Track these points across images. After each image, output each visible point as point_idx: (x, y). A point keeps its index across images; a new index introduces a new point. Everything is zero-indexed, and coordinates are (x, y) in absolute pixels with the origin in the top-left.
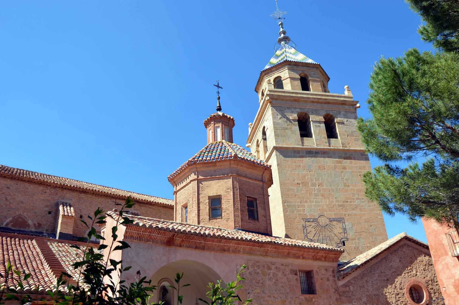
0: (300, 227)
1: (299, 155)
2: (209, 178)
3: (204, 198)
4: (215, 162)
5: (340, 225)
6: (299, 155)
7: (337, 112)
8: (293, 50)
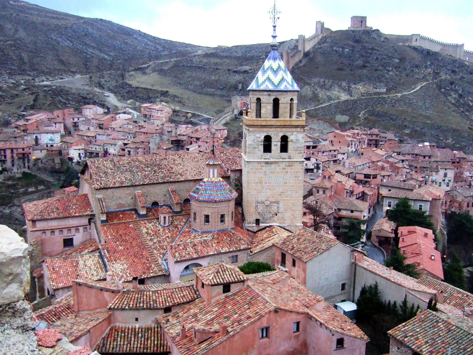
0: (254, 205)
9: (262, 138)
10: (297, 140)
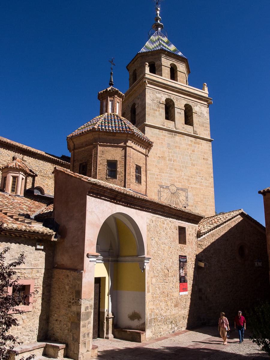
0: (156, 191)
1: (162, 134)
2: (109, 145)
3: (104, 161)
4: (115, 132)
5: (184, 194)
6: (162, 134)
7: (194, 104)
8: (166, 39)
9: (163, 100)
10: (201, 113)
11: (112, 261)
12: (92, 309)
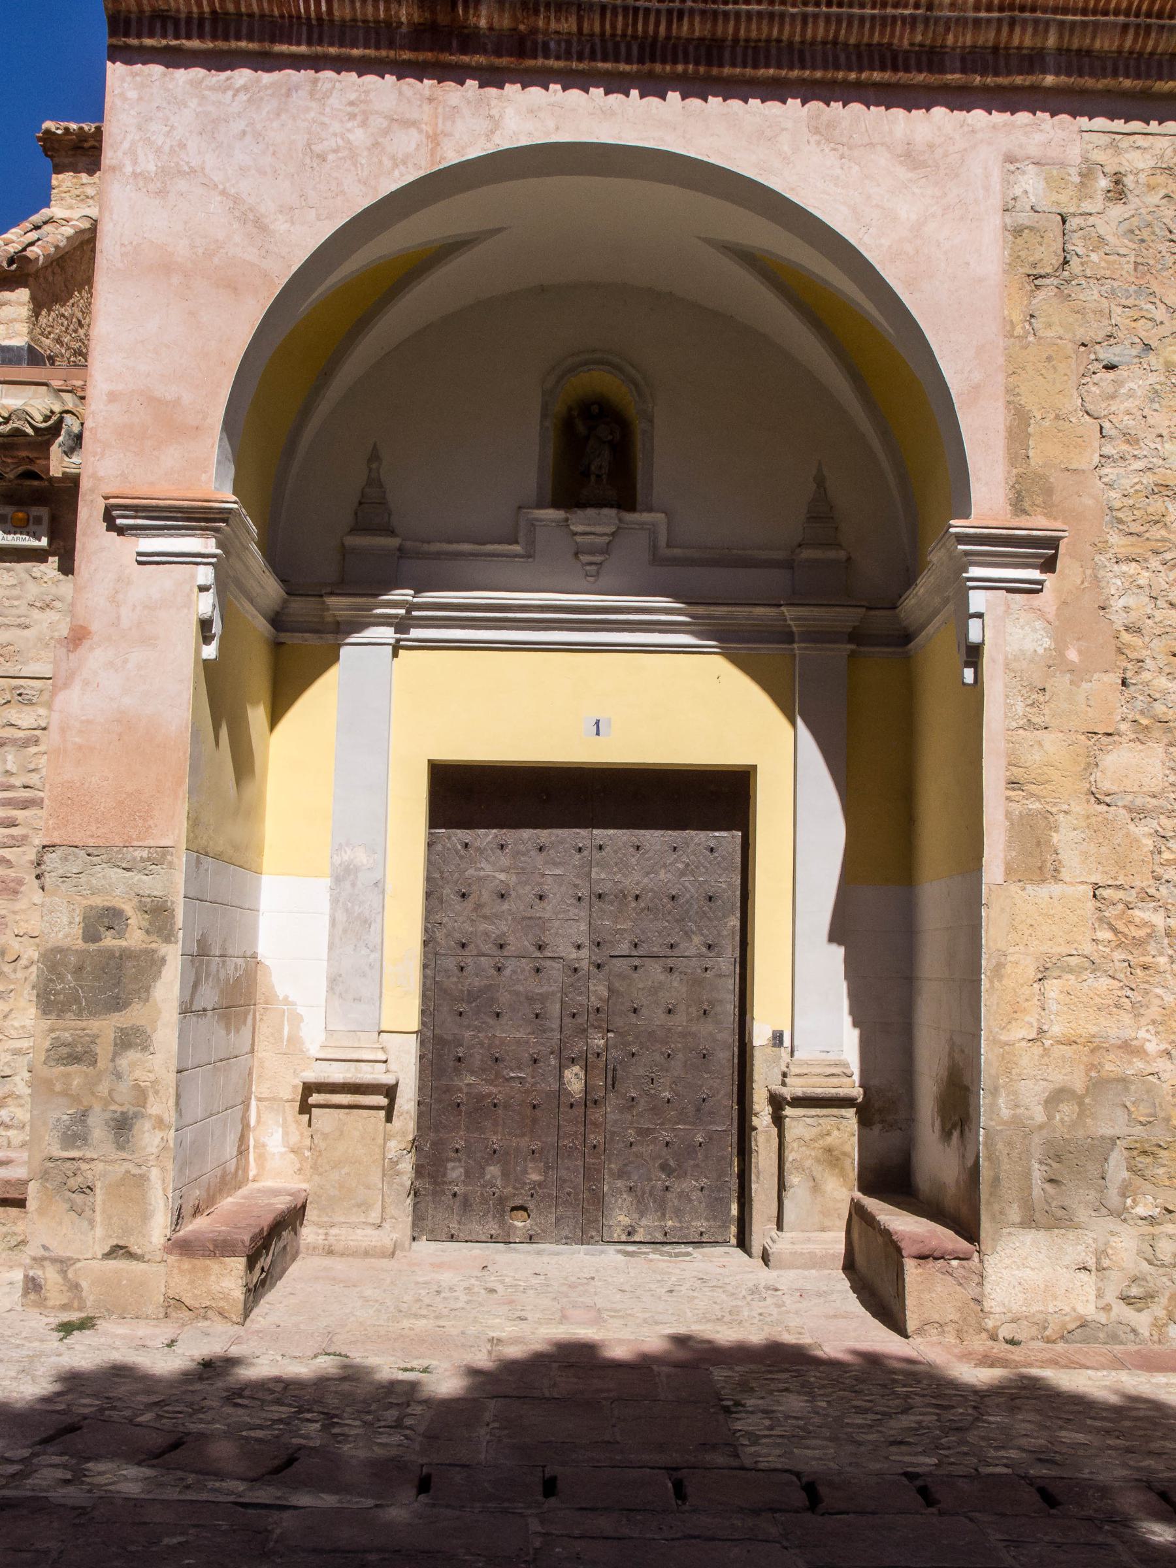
11: (816, 636)
12: (168, 939)
